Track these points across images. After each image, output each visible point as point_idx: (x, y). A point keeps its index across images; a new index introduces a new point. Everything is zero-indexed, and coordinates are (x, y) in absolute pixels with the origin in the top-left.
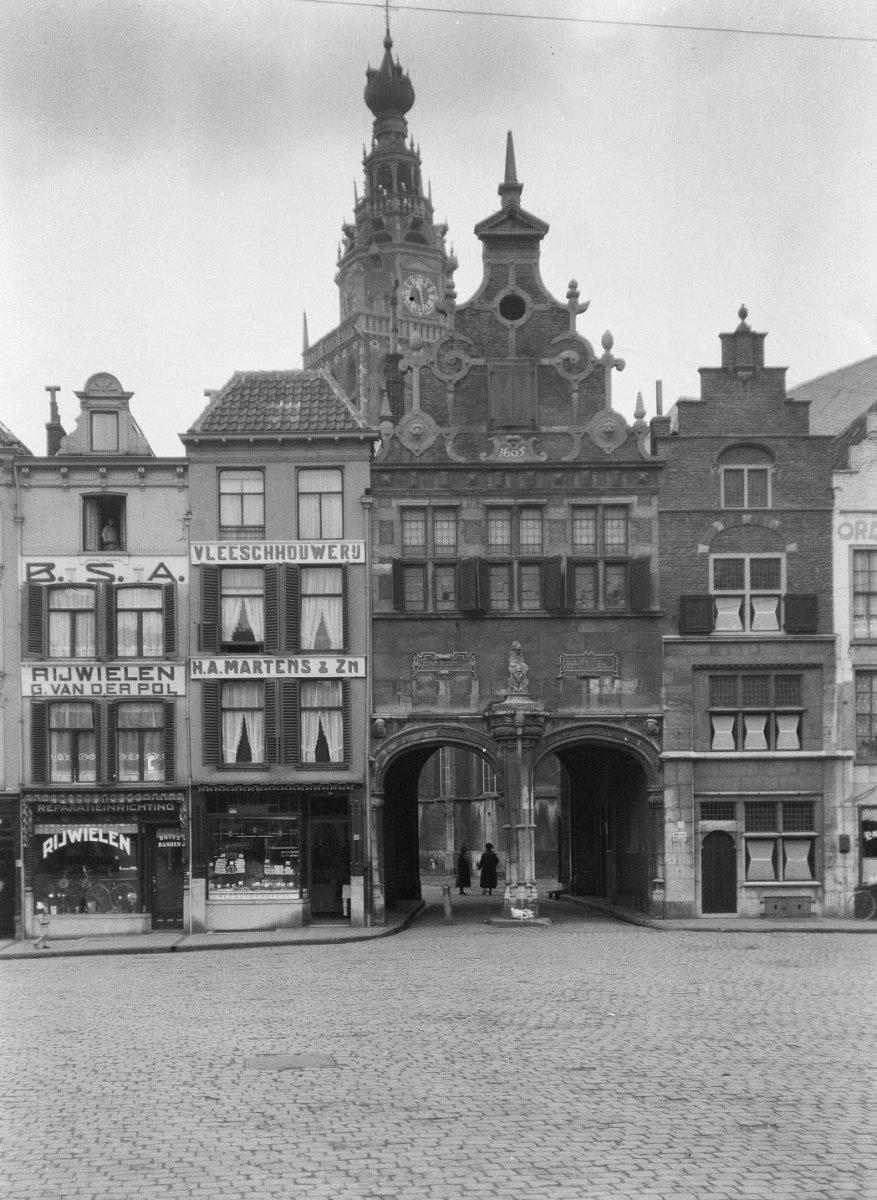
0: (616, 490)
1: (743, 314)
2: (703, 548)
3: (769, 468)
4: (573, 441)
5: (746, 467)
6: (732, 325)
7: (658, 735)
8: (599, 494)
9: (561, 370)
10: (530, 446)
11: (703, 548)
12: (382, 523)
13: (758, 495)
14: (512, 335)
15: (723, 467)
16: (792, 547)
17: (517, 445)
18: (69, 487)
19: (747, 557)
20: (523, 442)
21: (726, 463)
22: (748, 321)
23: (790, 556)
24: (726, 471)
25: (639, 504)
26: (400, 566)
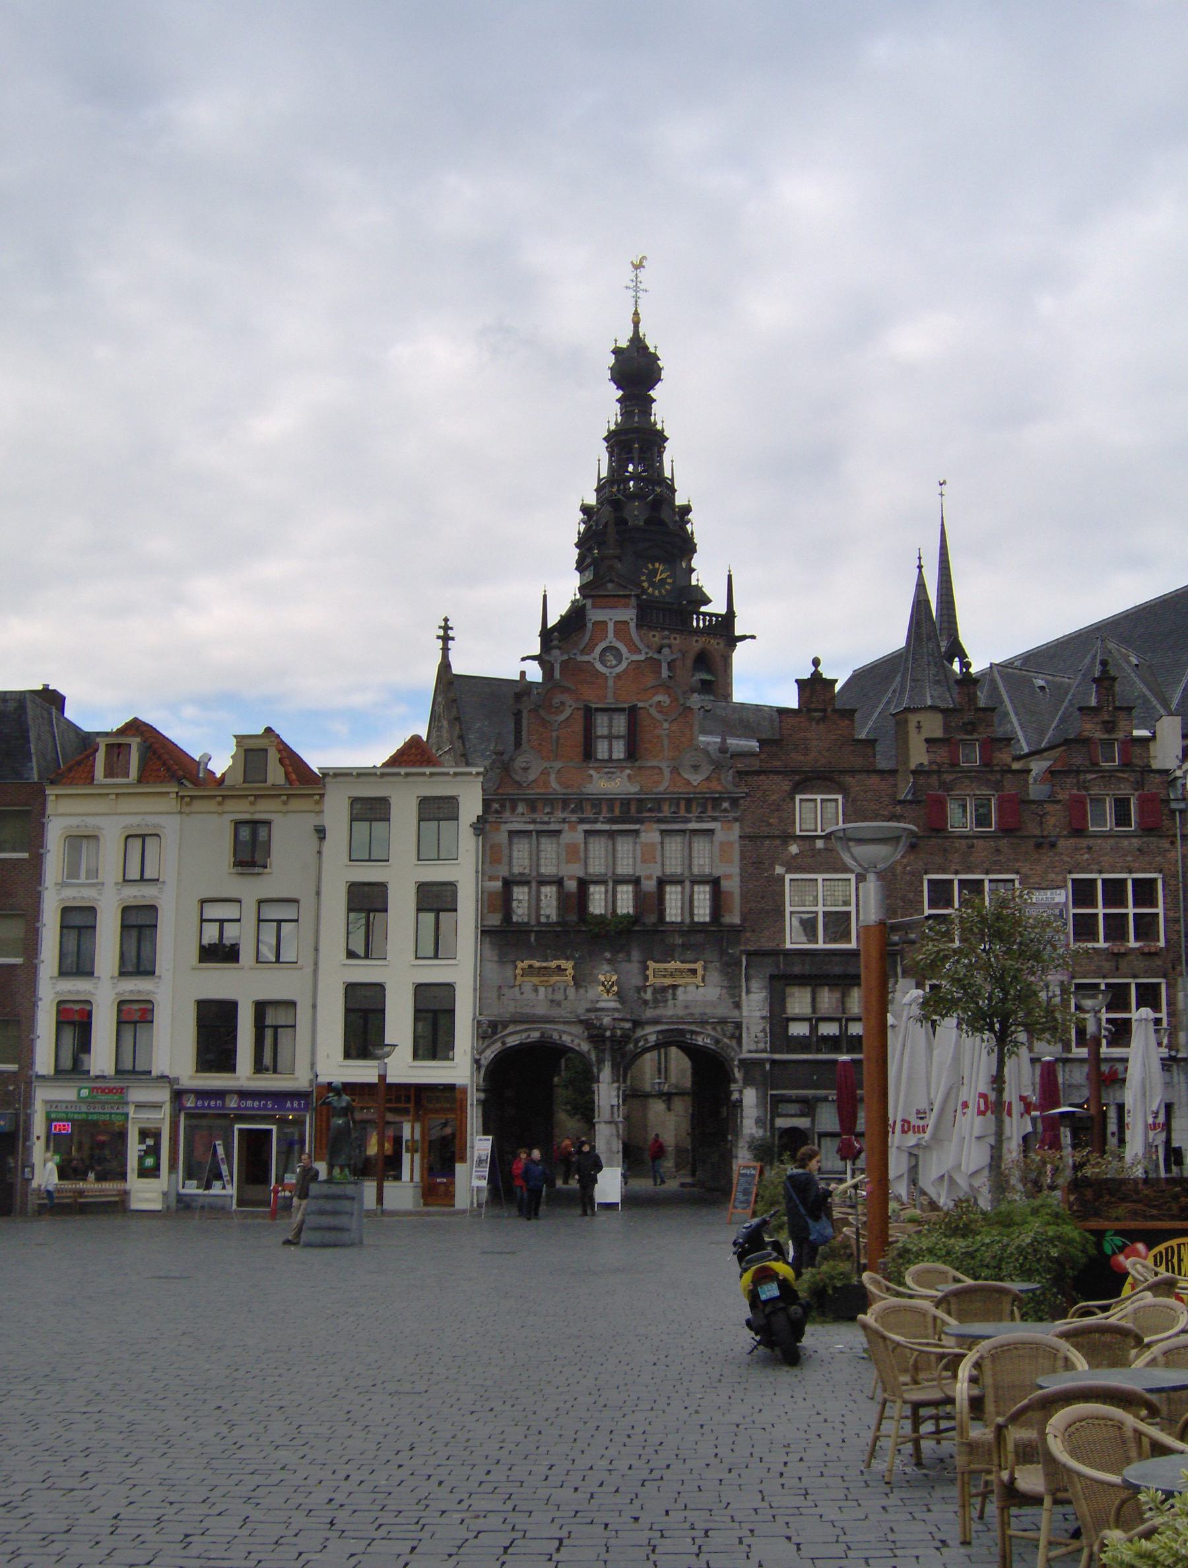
0: (700, 819)
1: (816, 662)
2: (779, 870)
3: (840, 797)
4: (662, 773)
5: (819, 797)
8: (688, 821)
9: (653, 711)
10: (626, 779)
11: (779, 870)
15: (798, 797)
17: (614, 776)
18: (223, 813)
19: (820, 877)
20: (618, 774)
22: (819, 669)
24: (801, 800)
25: (722, 829)
26: (508, 884)
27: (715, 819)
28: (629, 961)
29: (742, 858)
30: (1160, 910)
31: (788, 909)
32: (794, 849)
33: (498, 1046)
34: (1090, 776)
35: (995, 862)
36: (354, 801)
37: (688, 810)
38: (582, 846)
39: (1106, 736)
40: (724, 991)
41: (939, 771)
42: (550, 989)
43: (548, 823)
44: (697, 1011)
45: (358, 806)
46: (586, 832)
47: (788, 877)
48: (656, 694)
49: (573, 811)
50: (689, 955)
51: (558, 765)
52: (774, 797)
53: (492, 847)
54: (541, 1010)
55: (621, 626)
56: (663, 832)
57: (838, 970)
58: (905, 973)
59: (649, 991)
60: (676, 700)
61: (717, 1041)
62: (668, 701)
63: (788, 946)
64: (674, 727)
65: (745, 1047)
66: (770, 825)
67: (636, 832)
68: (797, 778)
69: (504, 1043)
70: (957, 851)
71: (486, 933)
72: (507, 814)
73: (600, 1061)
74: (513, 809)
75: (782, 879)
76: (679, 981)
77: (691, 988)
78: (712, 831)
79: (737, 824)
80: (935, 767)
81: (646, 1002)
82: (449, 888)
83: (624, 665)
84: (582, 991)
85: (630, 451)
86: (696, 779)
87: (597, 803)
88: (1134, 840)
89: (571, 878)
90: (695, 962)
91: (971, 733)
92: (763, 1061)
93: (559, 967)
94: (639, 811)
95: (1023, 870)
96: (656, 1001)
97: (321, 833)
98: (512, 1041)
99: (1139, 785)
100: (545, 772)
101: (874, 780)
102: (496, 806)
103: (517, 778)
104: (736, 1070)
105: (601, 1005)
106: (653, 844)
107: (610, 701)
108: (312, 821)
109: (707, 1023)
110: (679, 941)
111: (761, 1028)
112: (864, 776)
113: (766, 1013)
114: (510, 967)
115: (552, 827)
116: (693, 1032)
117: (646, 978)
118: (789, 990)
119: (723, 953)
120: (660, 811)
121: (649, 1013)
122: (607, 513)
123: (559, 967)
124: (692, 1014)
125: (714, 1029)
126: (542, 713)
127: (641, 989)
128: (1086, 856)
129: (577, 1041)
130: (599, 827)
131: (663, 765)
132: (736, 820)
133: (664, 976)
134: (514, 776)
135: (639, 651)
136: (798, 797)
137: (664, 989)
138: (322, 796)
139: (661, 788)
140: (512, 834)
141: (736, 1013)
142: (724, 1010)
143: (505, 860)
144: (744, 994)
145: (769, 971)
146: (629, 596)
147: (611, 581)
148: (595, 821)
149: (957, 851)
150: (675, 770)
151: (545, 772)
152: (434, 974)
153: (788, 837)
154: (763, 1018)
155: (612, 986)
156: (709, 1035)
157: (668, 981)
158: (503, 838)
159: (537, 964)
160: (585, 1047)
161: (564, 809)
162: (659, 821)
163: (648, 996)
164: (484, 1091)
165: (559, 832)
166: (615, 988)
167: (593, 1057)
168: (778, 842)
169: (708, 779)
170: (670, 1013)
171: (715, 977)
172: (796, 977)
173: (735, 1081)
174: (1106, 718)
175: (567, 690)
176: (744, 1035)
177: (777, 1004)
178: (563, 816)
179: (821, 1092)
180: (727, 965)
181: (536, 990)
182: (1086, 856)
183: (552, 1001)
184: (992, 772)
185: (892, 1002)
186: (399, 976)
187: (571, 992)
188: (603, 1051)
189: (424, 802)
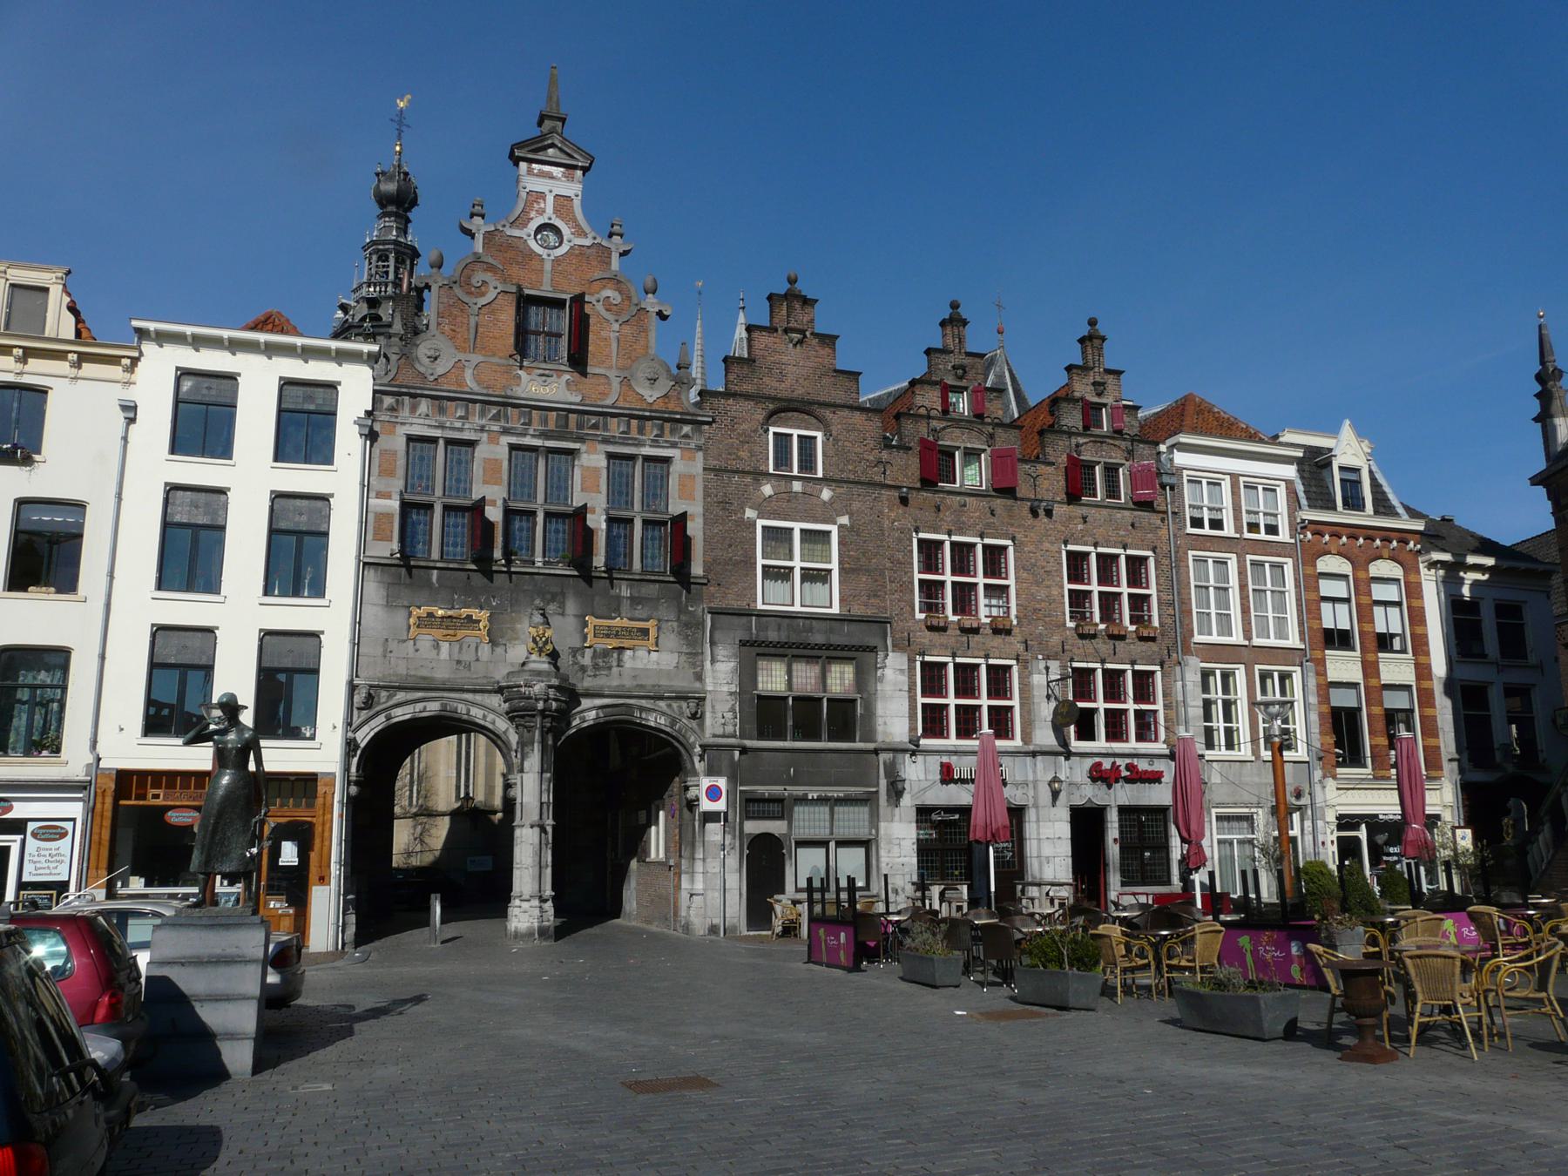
0: (655, 443)
2: (750, 513)
5: (796, 432)
6: (782, 288)
7: (697, 716)
8: (640, 444)
11: (750, 513)
12: (383, 453)
13: (807, 462)
14: (548, 267)
15: (772, 429)
16: (844, 520)
19: (797, 527)
21: (774, 425)
23: (841, 527)
27: (674, 445)
28: (563, 614)
29: (707, 495)
30: (1152, 591)
31: (760, 562)
32: (767, 490)
33: (378, 723)
34: (1081, 440)
35: (988, 525)
36: (183, 373)
37: (641, 431)
38: (505, 463)
39: (1096, 400)
40: (683, 658)
41: (929, 417)
42: (456, 647)
43: (461, 430)
44: (649, 682)
45: (187, 385)
46: (513, 447)
47: (760, 523)
48: (604, 287)
49: (496, 418)
50: (640, 611)
51: (476, 358)
52: (744, 426)
53: (383, 453)
54: (442, 674)
55: (562, 203)
56: (611, 456)
57: (819, 638)
58: (897, 648)
59: (589, 653)
60: (629, 298)
61: (673, 722)
62: (619, 299)
63: (760, 606)
64: (627, 330)
65: (708, 732)
66: (738, 458)
67: (572, 453)
68: (771, 406)
69: (388, 718)
70: (949, 508)
71: (366, 565)
72: (405, 413)
73: (524, 744)
74: (414, 409)
75: (754, 525)
76: (626, 643)
77: (641, 653)
78: (667, 460)
79: (700, 455)
80: (922, 411)
81: (583, 669)
82: (320, 504)
83: (565, 248)
84: (499, 650)
85: (387, 259)
86: (651, 395)
87: (530, 408)
88: (1127, 513)
89: (493, 503)
90: (647, 620)
91: (961, 378)
92: (733, 747)
93: (469, 617)
94: (580, 426)
95: (1018, 536)
96: (596, 667)
97: (130, 411)
98: (401, 714)
99: (1130, 454)
100: (459, 366)
101: (858, 418)
102: (388, 401)
103: (422, 369)
104: (696, 759)
105: (532, 666)
106: (596, 470)
107: (546, 290)
108: (118, 393)
109: (661, 698)
110: (625, 591)
111: (729, 706)
112: (846, 413)
113: (734, 688)
114: (403, 613)
115: (466, 436)
116: (642, 709)
117: (585, 638)
118: (762, 664)
119: (681, 610)
120: (606, 428)
121: (587, 683)
122: (363, 310)
123: (469, 617)
124: (641, 686)
125: (669, 706)
126: (457, 291)
127: (574, 652)
128: (1080, 527)
129: (491, 717)
130: (528, 441)
131: (612, 374)
132: (699, 448)
133: (608, 636)
134: (417, 365)
135: (586, 235)
136: (772, 429)
137: (606, 654)
138: (135, 361)
139: (609, 402)
140: (411, 439)
141: (697, 685)
142: (684, 683)
143: (401, 472)
144: (708, 664)
145: (741, 635)
146: (575, 167)
147: (552, 145)
148: (525, 435)
149: (949, 508)
150: (626, 381)
151: (459, 366)
152: (292, 615)
153: (760, 475)
154: (731, 694)
155: (546, 643)
156: (664, 714)
157: (613, 643)
158: (400, 443)
159: (440, 612)
160: (502, 725)
161: (483, 414)
162: (606, 441)
163: (587, 660)
164: (357, 783)
165: (472, 444)
166: (549, 647)
167: (513, 738)
168: (748, 479)
169: (665, 396)
170: (615, 683)
171: (671, 640)
172: (769, 644)
173: (695, 774)
174: (1098, 379)
175: (491, 268)
176: (708, 715)
177: (747, 675)
178: (484, 422)
179: (798, 790)
180: (687, 625)
181: (437, 647)
182: (1080, 527)
183: (459, 662)
184: (983, 423)
185: (881, 679)
186: (239, 617)
187: (485, 649)
188: (530, 729)
189: (287, 384)
